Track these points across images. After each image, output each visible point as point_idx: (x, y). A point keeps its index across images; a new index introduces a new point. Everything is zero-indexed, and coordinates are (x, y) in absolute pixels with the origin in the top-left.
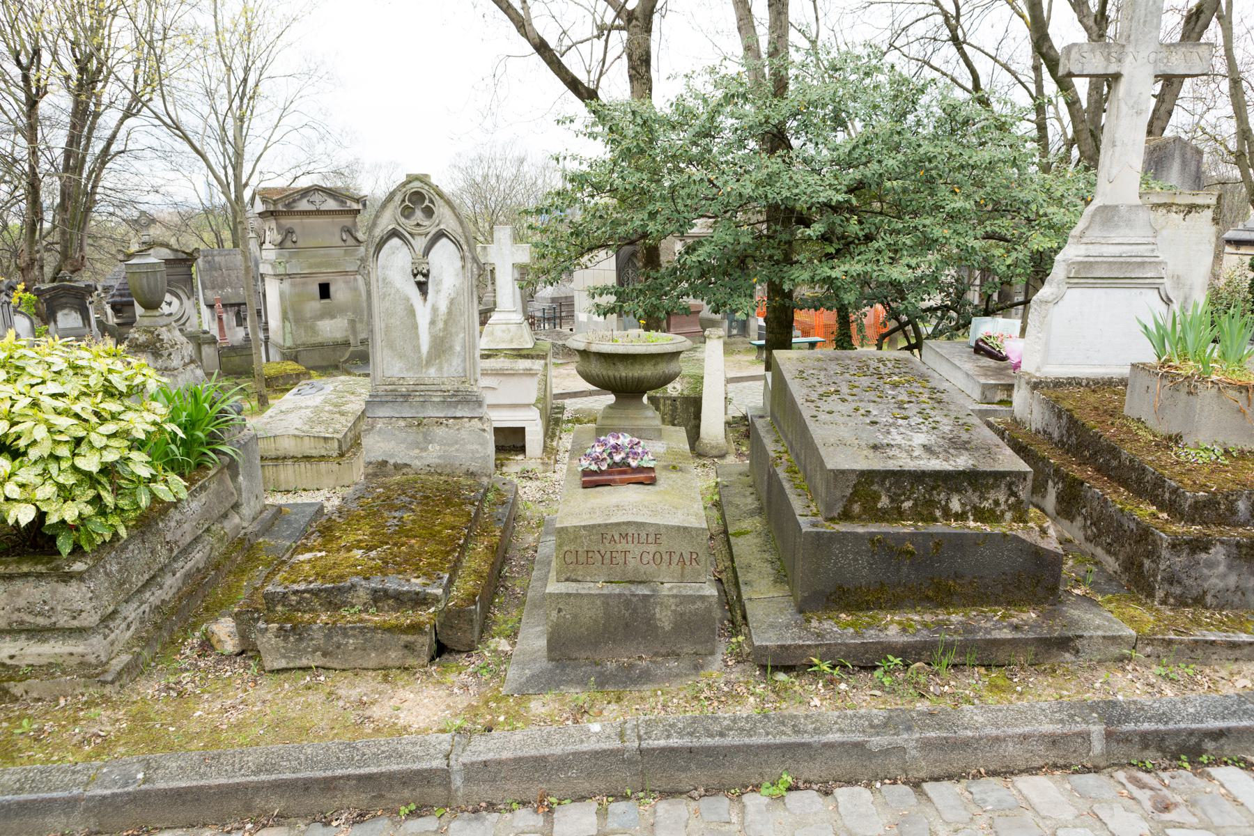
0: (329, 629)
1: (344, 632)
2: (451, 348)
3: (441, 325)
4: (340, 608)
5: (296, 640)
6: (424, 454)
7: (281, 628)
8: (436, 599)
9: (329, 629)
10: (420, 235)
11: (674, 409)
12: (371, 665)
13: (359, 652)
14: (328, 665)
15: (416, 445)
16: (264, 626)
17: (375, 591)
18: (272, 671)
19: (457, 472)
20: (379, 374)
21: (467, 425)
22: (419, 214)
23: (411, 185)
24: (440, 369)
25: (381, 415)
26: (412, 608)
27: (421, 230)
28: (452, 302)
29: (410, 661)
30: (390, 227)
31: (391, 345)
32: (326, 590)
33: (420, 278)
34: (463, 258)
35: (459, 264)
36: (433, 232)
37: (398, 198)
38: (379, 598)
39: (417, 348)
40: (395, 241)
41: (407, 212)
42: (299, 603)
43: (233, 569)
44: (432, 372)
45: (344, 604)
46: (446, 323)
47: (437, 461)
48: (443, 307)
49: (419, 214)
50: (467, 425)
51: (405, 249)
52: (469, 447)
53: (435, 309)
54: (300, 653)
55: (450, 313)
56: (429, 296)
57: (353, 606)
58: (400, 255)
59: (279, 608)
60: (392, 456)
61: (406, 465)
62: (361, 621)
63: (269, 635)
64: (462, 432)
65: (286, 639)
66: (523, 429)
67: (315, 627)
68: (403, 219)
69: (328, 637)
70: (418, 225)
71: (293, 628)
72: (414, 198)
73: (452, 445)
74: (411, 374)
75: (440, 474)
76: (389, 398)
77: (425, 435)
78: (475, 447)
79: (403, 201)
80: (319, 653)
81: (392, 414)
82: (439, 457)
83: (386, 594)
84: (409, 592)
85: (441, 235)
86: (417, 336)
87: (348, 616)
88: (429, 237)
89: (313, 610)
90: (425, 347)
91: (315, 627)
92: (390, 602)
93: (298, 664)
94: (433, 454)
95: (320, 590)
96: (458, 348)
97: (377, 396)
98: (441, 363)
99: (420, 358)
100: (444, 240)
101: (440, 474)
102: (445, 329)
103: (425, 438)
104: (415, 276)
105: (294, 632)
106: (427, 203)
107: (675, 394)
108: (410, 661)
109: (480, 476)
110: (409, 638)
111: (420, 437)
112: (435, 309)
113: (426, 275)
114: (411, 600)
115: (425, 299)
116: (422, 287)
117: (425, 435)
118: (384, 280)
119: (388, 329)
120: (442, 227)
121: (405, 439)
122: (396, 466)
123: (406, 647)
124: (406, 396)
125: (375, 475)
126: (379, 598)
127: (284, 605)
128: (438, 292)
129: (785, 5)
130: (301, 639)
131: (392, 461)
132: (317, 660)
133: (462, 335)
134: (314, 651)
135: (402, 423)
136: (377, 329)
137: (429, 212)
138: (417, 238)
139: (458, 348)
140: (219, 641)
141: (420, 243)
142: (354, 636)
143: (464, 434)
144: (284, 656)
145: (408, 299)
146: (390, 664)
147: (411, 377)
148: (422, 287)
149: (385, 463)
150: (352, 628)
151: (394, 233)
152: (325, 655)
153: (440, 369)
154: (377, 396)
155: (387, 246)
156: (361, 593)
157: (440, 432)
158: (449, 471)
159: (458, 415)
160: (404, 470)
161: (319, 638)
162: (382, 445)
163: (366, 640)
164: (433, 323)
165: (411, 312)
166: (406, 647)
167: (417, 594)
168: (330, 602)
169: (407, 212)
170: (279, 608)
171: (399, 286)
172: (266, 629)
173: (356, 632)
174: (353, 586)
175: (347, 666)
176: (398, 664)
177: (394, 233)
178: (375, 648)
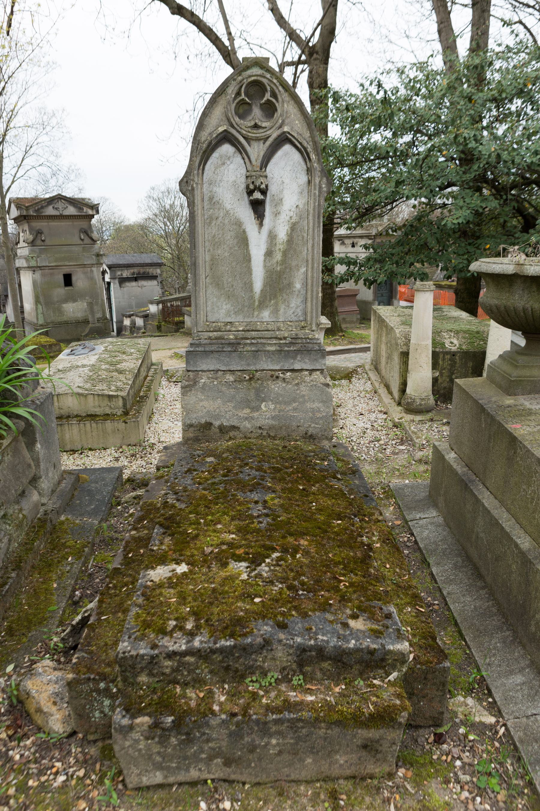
0: (238, 724)
1: (264, 728)
2: (290, 285)
3: (278, 256)
4: (243, 677)
5: (181, 742)
6: (256, 414)
7: (156, 725)
8: (401, 658)
9: (238, 724)
10: (258, 139)
11: (453, 364)
12: (304, 775)
13: (286, 757)
14: (233, 777)
15: (247, 403)
16: (126, 722)
17: (303, 650)
18: (138, 789)
19: (294, 435)
20: (202, 317)
21: (308, 379)
22: (257, 112)
23: (249, 72)
24: (276, 311)
25: (204, 367)
26: (361, 674)
27: (260, 133)
28: (293, 227)
29: (371, 768)
30: (221, 129)
31: (217, 283)
32: (222, 650)
33: (257, 195)
34: (309, 171)
35: (304, 178)
36: (275, 135)
37: (232, 90)
38: (308, 660)
39: (249, 286)
40: (227, 149)
41: (243, 109)
42: (175, 670)
43: (36, 562)
44: (266, 315)
45: (251, 670)
46: (285, 254)
47: (271, 422)
48: (282, 234)
49: (257, 112)
50: (308, 379)
51: (238, 159)
52: (309, 405)
53: (272, 237)
54: (186, 762)
55: (290, 240)
56: (267, 221)
57: (264, 674)
58: (232, 167)
59: (143, 678)
60: (217, 417)
61: (234, 428)
62: (288, 706)
63: (135, 735)
64: (302, 387)
65: (163, 740)
66: (480, 375)
67: (214, 722)
68: (237, 119)
69: (236, 736)
70: (256, 126)
71: (177, 725)
72: (252, 91)
73: (288, 403)
74: (240, 318)
75: (274, 438)
76: (214, 348)
77: (258, 392)
78: (316, 405)
79: (238, 94)
80: (219, 760)
81: (218, 367)
82: (273, 418)
83: (321, 653)
84: (357, 650)
85: (284, 139)
86: (249, 271)
87: (266, 692)
88: (268, 143)
89: (198, 682)
90: (258, 285)
91: (214, 722)
92: (326, 665)
93: (182, 777)
94: (267, 413)
95: (213, 651)
96: (298, 286)
97: (199, 345)
98: (276, 304)
99: (252, 297)
100: (287, 148)
101: (274, 438)
102: (284, 261)
103: (257, 395)
104: (250, 193)
105: (183, 727)
106: (268, 96)
107: (454, 349)
108: (371, 768)
109: (320, 439)
110: (372, 734)
111: (252, 395)
112: (272, 237)
113: (264, 192)
114: (360, 662)
115: (261, 225)
116: (258, 207)
117: (258, 392)
118: (211, 199)
119: (214, 262)
120: (286, 129)
121: (233, 397)
122: (222, 429)
123: (365, 747)
124: (235, 345)
125: (197, 440)
126: (308, 660)
127: (151, 674)
128: (277, 214)
129: (489, 3)
130: (189, 740)
131: (217, 423)
132: (217, 770)
133: (303, 270)
134: (211, 758)
135: (230, 378)
136: (200, 261)
137: (270, 109)
138: (255, 144)
139: (298, 286)
140: (39, 710)
141: (257, 151)
142: (279, 733)
143: (304, 390)
144: (159, 767)
145: (239, 224)
146: (336, 772)
147: (240, 321)
148: (258, 207)
149: (209, 425)
150: (277, 722)
151: (226, 138)
152: (228, 763)
153: (276, 311)
154: (199, 345)
155: (215, 155)
156: (280, 653)
157: (276, 387)
158: (284, 433)
159: (297, 366)
160: (232, 434)
161: (218, 736)
162: (205, 403)
163: (299, 739)
164: (269, 254)
165: (243, 240)
166: (365, 747)
167: (372, 652)
168: (227, 669)
169: (243, 109)
170: (143, 678)
171: (228, 206)
172: (131, 728)
173: (283, 727)
174: (267, 643)
175: (263, 778)
176: (348, 772)
177: (226, 138)
178: (313, 751)
